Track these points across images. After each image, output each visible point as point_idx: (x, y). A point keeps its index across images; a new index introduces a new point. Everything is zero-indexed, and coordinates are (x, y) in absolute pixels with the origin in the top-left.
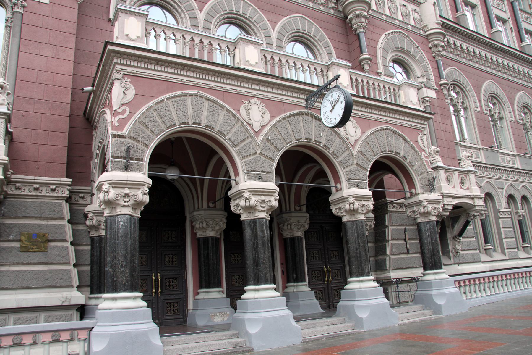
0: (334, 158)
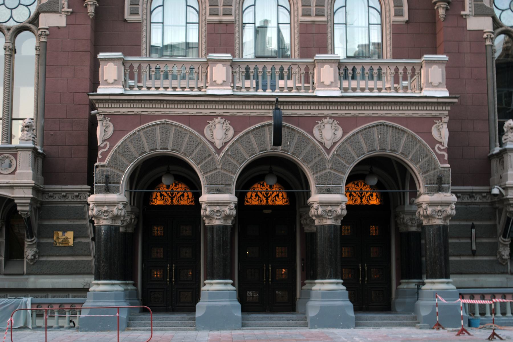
0: (303, 164)
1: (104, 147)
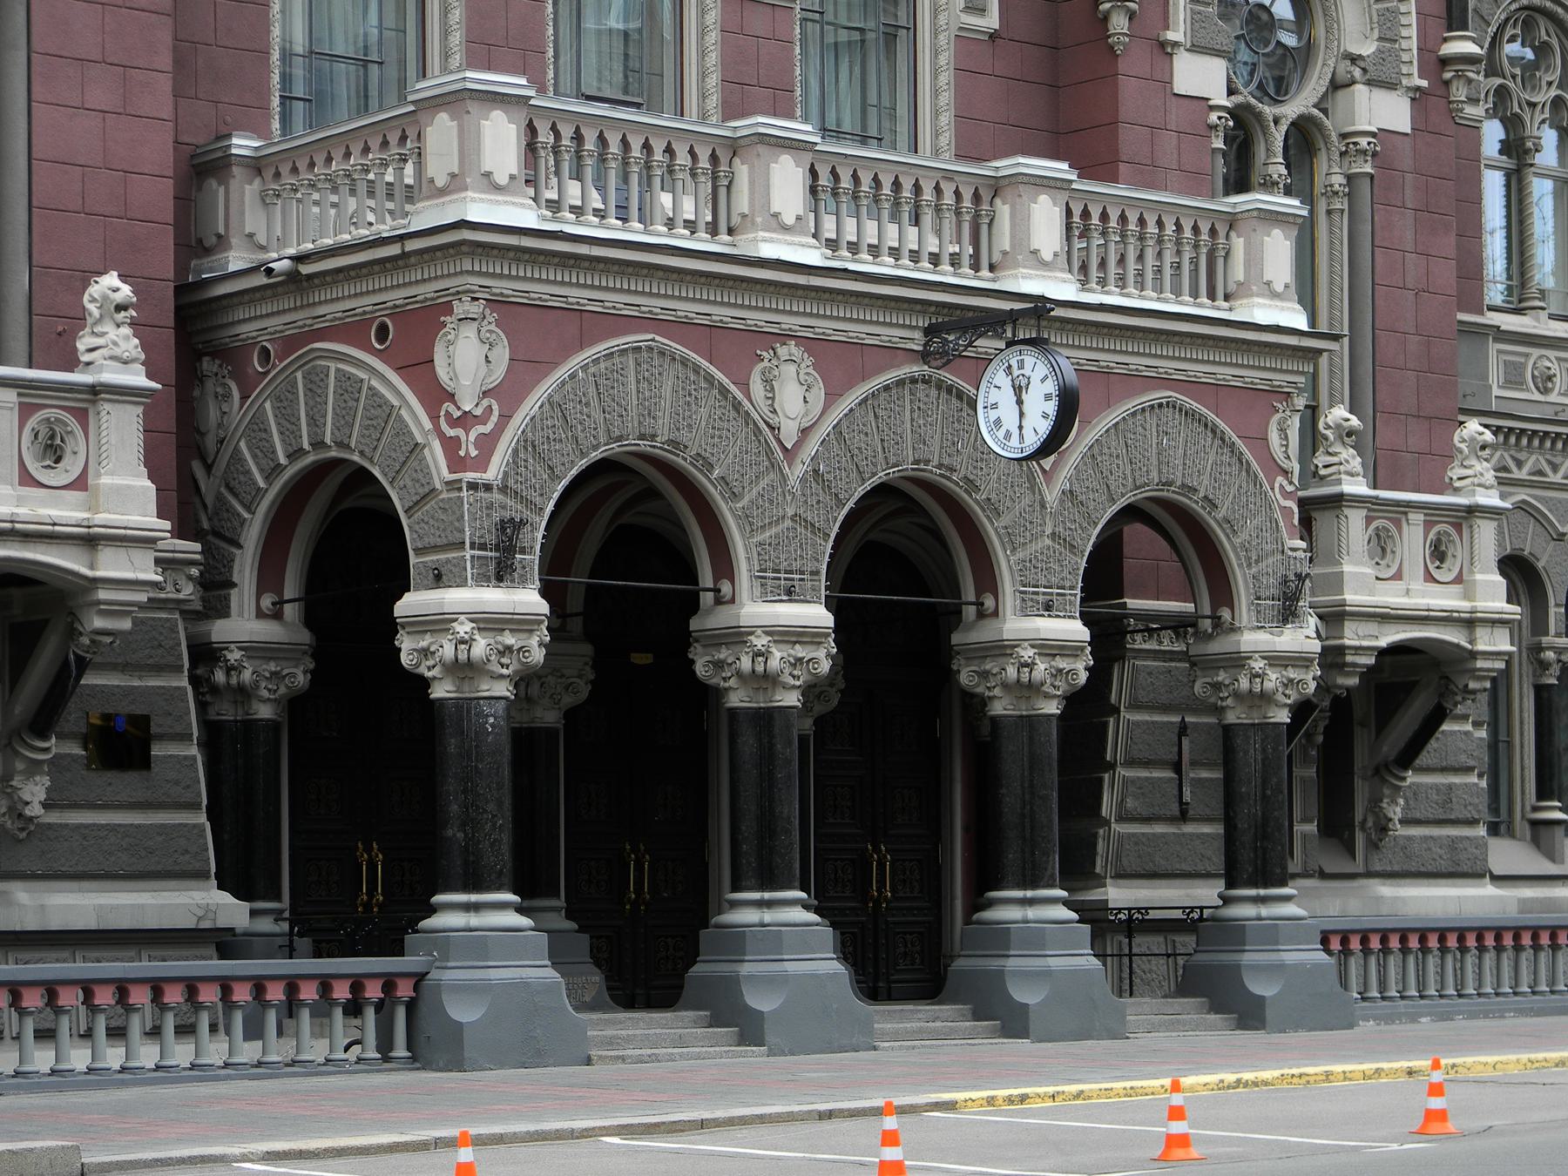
0: (988, 517)
1: (482, 420)
